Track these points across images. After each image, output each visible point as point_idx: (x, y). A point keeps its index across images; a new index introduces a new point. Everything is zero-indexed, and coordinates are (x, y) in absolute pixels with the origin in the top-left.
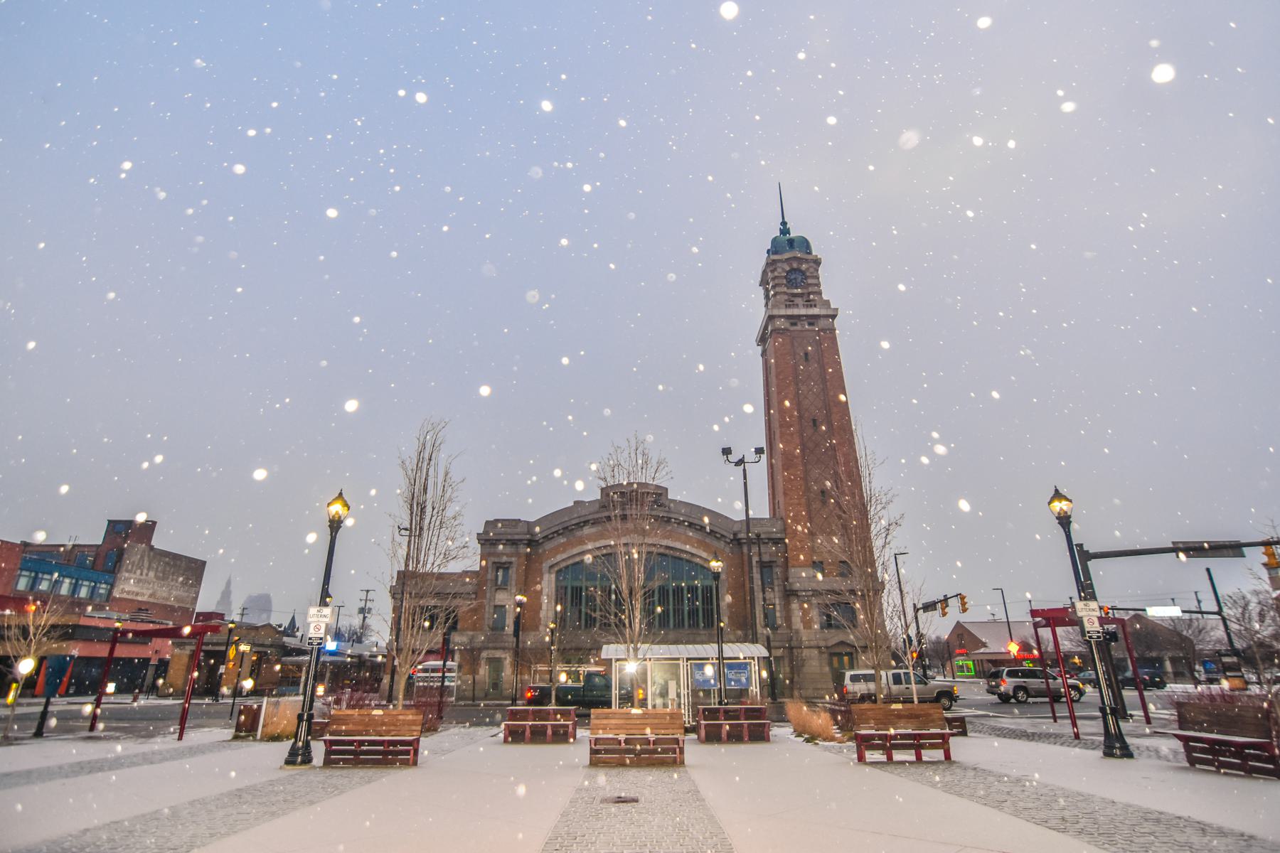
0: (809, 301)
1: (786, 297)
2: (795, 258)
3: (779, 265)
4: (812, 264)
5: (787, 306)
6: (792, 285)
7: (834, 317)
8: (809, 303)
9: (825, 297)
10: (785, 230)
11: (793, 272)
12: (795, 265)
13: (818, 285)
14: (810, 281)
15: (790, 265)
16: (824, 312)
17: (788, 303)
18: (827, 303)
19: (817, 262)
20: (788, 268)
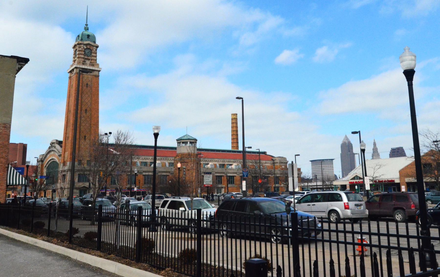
0: (91, 63)
1: (83, 60)
2: (89, 44)
3: (82, 45)
4: (95, 48)
5: (83, 64)
6: (86, 55)
7: (99, 71)
8: (91, 64)
9: (98, 62)
10: (87, 29)
11: (87, 49)
12: (88, 47)
13: (96, 57)
14: (93, 54)
15: (86, 46)
16: (96, 69)
17: (84, 63)
18: (98, 65)
19: (97, 47)
20: (85, 47)
